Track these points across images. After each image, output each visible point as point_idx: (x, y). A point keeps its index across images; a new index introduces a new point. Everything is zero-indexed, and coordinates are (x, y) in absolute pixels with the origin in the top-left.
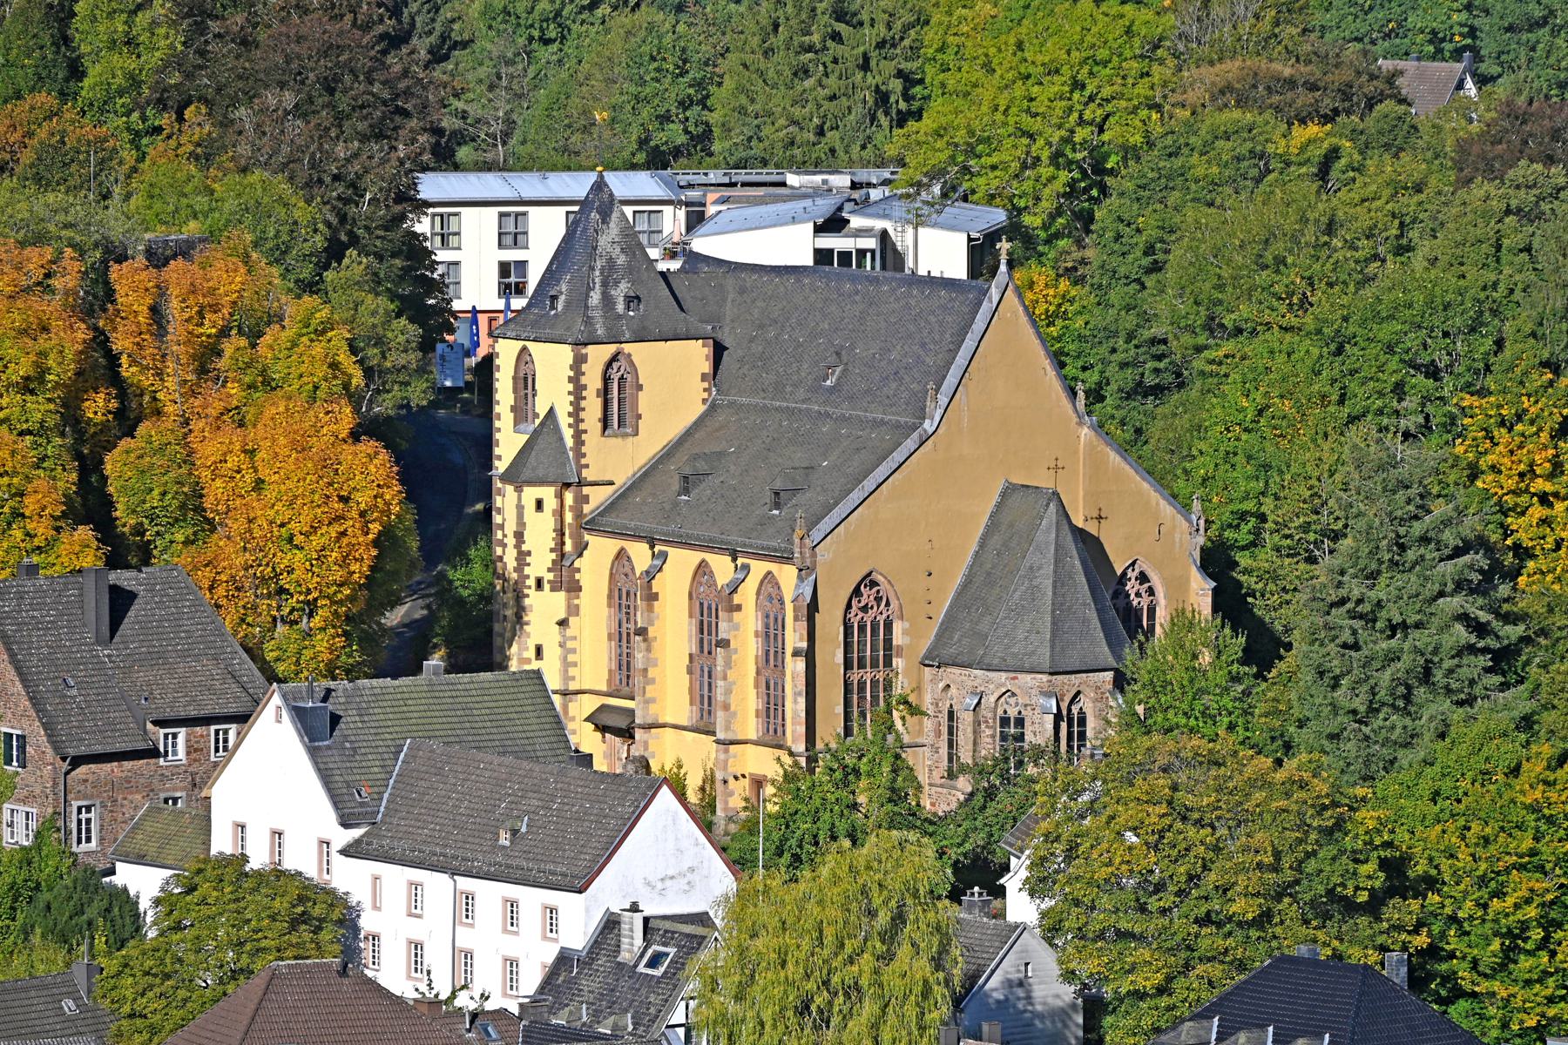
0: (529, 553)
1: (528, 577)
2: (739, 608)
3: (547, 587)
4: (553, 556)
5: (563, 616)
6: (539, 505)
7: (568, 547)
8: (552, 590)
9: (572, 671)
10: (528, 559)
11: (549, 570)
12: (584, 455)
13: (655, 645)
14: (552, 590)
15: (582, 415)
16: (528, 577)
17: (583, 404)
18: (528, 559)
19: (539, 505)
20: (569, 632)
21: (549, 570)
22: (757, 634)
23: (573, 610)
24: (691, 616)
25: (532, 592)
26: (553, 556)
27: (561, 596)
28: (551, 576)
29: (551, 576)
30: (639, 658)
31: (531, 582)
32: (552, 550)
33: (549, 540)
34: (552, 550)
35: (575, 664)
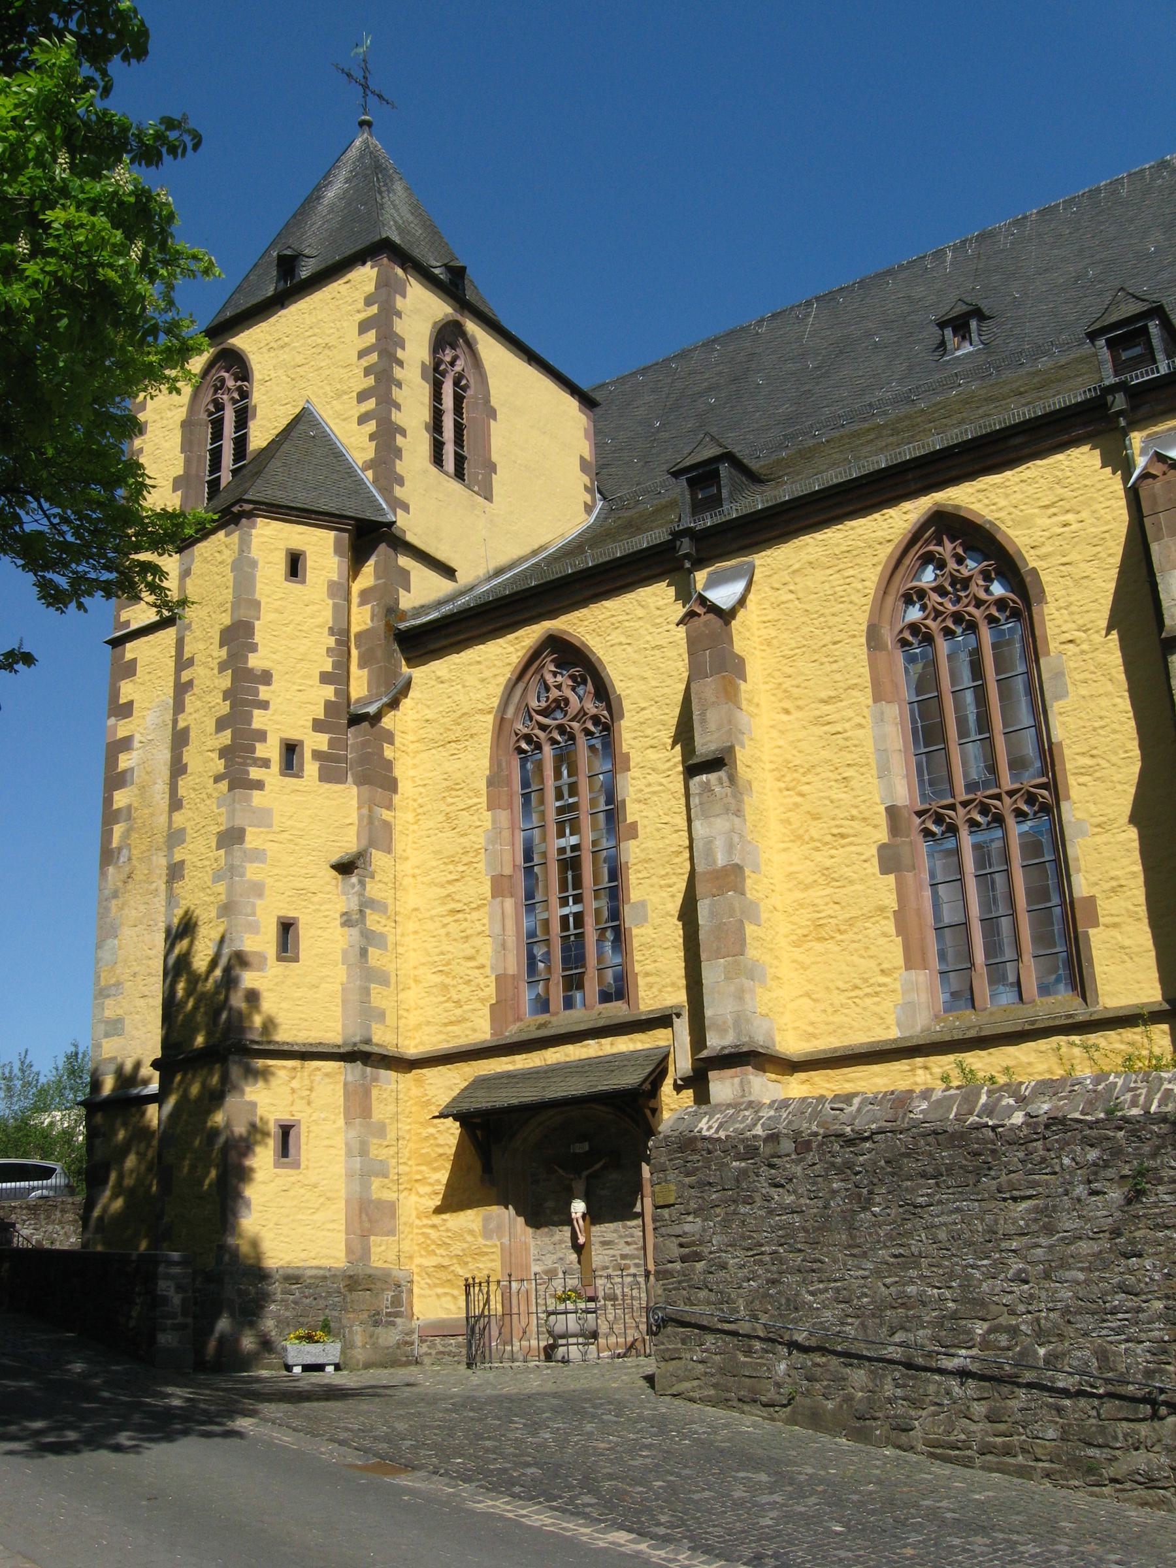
3: (311, 768)
4: (329, 692)
5: (348, 844)
6: (295, 565)
8: (327, 776)
10: (264, 692)
11: (318, 726)
14: (327, 776)
16: (262, 736)
18: (264, 692)
19: (295, 565)
20: (374, 889)
21: (318, 726)
26: (329, 692)
27: (345, 800)
29: (321, 741)
31: (271, 750)
32: (325, 678)
34: (325, 678)
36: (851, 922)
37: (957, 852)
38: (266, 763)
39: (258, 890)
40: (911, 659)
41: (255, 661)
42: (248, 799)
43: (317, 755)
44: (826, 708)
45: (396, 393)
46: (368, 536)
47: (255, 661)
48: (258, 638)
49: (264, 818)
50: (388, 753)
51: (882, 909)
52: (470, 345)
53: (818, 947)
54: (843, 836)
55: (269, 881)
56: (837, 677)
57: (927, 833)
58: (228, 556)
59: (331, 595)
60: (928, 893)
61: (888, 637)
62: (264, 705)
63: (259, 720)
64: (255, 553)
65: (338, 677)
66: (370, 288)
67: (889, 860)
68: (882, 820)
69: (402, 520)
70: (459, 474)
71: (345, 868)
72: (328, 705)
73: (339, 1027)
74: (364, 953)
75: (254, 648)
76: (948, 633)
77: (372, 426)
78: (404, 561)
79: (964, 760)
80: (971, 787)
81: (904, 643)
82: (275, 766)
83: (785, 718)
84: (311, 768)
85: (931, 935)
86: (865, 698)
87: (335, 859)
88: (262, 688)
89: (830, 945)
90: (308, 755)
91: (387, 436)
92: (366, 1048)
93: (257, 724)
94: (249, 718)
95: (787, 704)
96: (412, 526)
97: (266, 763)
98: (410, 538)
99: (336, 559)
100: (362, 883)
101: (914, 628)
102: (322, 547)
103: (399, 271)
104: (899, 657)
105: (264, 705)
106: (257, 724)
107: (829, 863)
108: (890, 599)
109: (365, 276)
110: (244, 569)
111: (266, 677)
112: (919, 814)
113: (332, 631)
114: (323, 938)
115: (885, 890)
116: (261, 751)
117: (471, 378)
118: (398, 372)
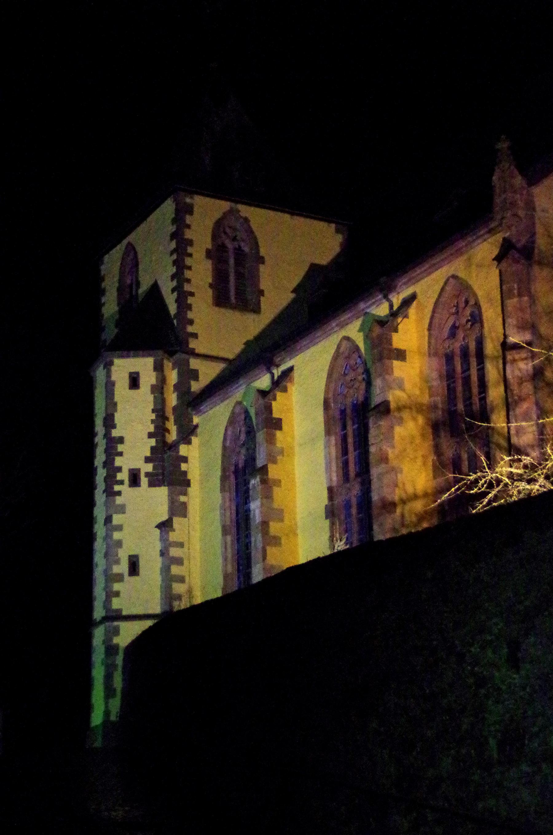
1: (119, 469)
3: (144, 481)
4: (153, 442)
6: (134, 382)
8: (152, 484)
10: (120, 448)
11: (147, 460)
14: (152, 484)
16: (119, 469)
17: (188, 261)
18: (120, 448)
19: (134, 382)
21: (147, 460)
23: (178, 509)
26: (153, 442)
27: (162, 492)
28: (149, 468)
29: (149, 468)
31: (124, 476)
32: (150, 435)
34: (150, 435)
38: (121, 482)
41: (115, 433)
43: (147, 474)
45: (188, 274)
47: (115, 433)
49: (122, 509)
59: (153, 392)
62: (121, 454)
63: (118, 462)
72: (152, 448)
75: (114, 427)
84: (144, 481)
97: (121, 482)
105: (121, 454)
111: (121, 440)
116: (119, 476)
118: (188, 261)
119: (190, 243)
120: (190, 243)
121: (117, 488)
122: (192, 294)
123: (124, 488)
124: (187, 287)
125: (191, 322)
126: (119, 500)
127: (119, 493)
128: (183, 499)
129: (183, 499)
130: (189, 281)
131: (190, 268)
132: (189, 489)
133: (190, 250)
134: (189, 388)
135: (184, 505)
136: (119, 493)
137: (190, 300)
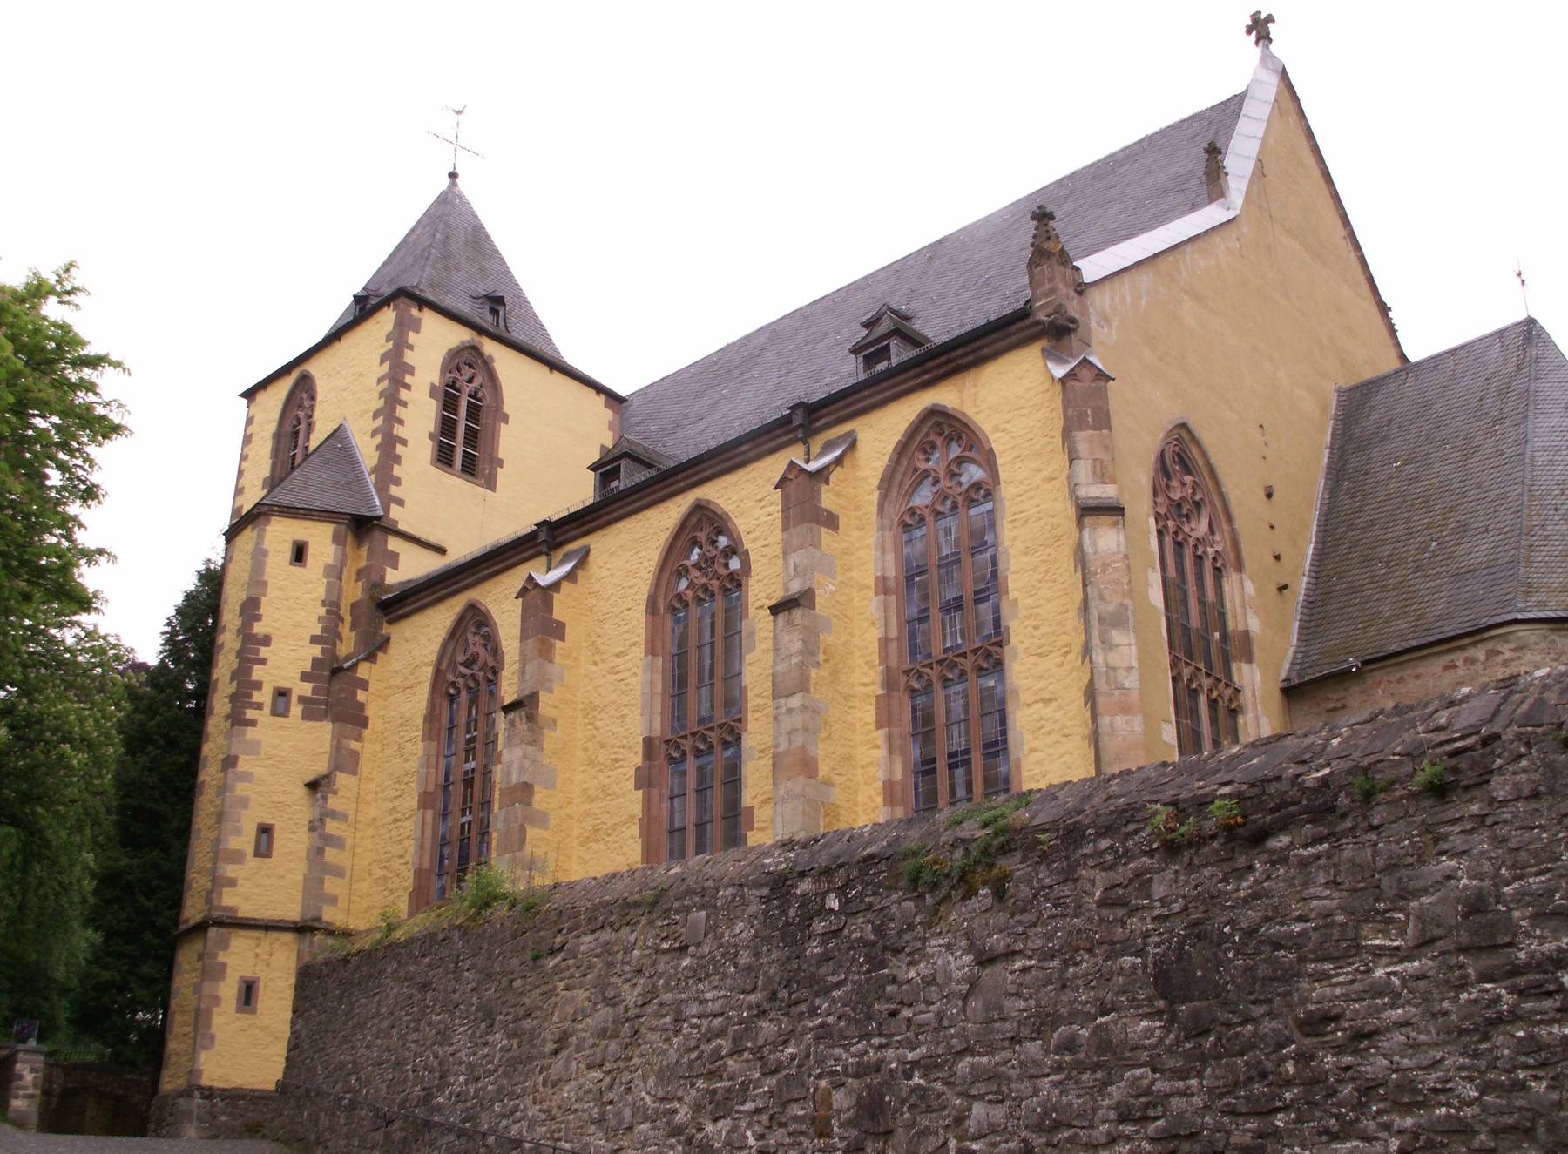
0: (266, 640)
1: (258, 685)
2: (831, 521)
4: (317, 651)
5: (320, 767)
6: (299, 553)
7: (346, 647)
8: (306, 716)
9: (331, 885)
10: (264, 652)
11: (305, 677)
12: (397, 482)
13: (550, 739)
14: (306, 716)
15: (401, 412)
16: (258, 685)
17: (404, 394)
18: (264, 652)
19: (299, 553)
20: (333, 803)
21: (305, 677)
22: (882, 587)
23: (345, 760)
24: (652, 649)
25: (263, 717)
26: (317, 651)
27: (322, 733)
28: (307, 689)
29: (307, 689)
30: (511, 761)
31: (264, 696)
32: (315, 640)
33: (311, 620)
34: (315, 640)
35: (338, 872)
36: (614, 827)
37: (684, 773)
38: (260, 706)
39: (244, 803)
40: (678, 621)
41: (259, 628)
42: (244, 734)
43: (302, 699)
44: (619, 661)
45: (401, 412)
46: (363, 527)
47: (259, 628)
48: (262, 611)
49: (254, 748)
50: (361, 696)
51: (632, 817)
52: (487, 365)
53: (594, 846)
54: (616, 760)
55: (253, 796)
56: (626, 636)
57: (672, 759)
58: (250, 547)
59: (326, 575)
60: (666, 805)
61: (662, 606)
62: (263, 662)
63: (258, 673)
64: (267, 545)
65: (328, 637)
66: (389, 327)
67: (644, 780)
68: (640, 748)
69: (395, 512)
70: (470, 468)
71: (313, 786)
72: (315, 661)
73: (299, 909)
74: (320, 851)
75: (258, 618)
76: (700, 601)
77: (378, 439)
78: (393, 544)
79: (698, 703)
80: (701, 721)
81: (674, 609)
82: (267, 710)
83: (594, 668)
84: (296, 710)
85: (665, 838)
86: (639, 651)
87: (309, 779)
88: (263, 649)
89: (602, 846)
90: (294, 699)
91: (389, 447)
92: (316, 925)
93: (255, 677)
94: (250, 671)
95: (596, 658)
96: (401, 517)
97: (260, 706)
98: (402, 526)
99: (334, 547)
100: (325, 798)
101: (679, 596)
102: (321, 539)
103: (415, 312)
104: (669, 621)
105: (263, 662)
106: (255, 677)
107: (607, 781)
108: (666, 575)
109: (387, 317)
110: (260, 555)
111: (266, 640)
112: (667, 742)
113: (324, 603)
114: (292, 841)
115: (634, 802)
116: (257, 697)
117: (485, 393)
118: (404, 394)
119: (411, 370)
120: (411, 370)
121: (250, 714)
122: (404, 442)
123: (263, 717)
124: (398, 430)
125: (397, 482)
126: (250, 733)
127: (253, 723)
128: (354, 745)
129: (354, 745)
130: (401, 422)
131: (404, 404)
132: (366, 733)
133: (408, 379)
134: (383, 578)
135: (355, 755)
136: (253, 723)
137: (400, 449)
